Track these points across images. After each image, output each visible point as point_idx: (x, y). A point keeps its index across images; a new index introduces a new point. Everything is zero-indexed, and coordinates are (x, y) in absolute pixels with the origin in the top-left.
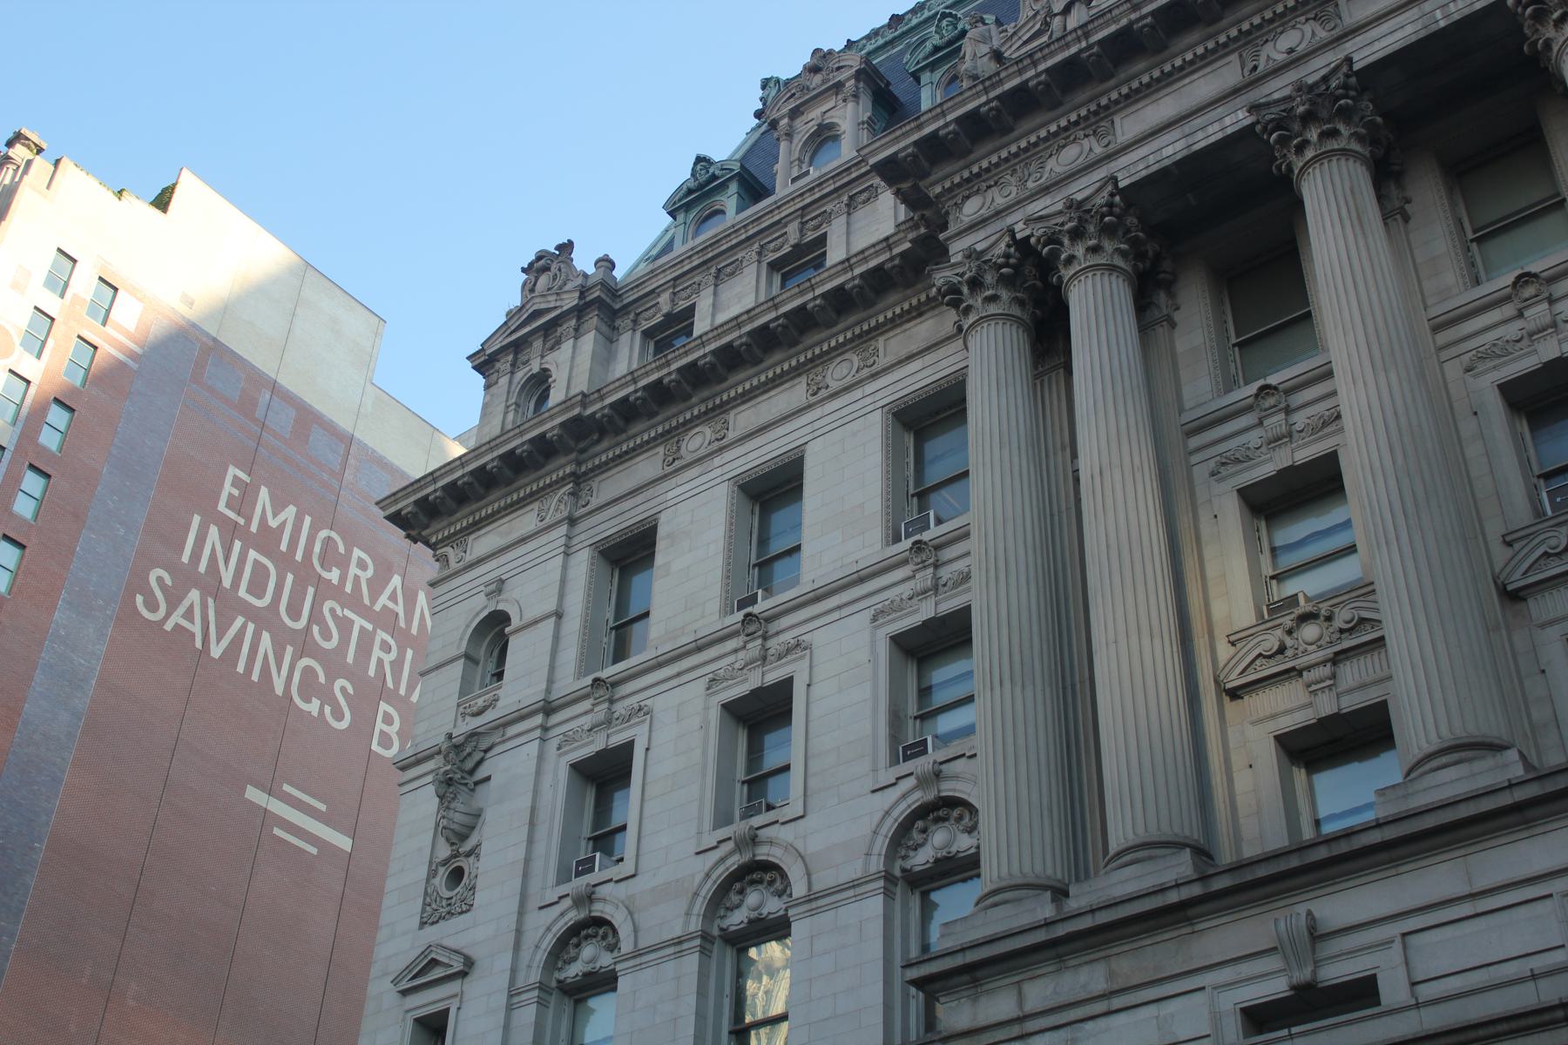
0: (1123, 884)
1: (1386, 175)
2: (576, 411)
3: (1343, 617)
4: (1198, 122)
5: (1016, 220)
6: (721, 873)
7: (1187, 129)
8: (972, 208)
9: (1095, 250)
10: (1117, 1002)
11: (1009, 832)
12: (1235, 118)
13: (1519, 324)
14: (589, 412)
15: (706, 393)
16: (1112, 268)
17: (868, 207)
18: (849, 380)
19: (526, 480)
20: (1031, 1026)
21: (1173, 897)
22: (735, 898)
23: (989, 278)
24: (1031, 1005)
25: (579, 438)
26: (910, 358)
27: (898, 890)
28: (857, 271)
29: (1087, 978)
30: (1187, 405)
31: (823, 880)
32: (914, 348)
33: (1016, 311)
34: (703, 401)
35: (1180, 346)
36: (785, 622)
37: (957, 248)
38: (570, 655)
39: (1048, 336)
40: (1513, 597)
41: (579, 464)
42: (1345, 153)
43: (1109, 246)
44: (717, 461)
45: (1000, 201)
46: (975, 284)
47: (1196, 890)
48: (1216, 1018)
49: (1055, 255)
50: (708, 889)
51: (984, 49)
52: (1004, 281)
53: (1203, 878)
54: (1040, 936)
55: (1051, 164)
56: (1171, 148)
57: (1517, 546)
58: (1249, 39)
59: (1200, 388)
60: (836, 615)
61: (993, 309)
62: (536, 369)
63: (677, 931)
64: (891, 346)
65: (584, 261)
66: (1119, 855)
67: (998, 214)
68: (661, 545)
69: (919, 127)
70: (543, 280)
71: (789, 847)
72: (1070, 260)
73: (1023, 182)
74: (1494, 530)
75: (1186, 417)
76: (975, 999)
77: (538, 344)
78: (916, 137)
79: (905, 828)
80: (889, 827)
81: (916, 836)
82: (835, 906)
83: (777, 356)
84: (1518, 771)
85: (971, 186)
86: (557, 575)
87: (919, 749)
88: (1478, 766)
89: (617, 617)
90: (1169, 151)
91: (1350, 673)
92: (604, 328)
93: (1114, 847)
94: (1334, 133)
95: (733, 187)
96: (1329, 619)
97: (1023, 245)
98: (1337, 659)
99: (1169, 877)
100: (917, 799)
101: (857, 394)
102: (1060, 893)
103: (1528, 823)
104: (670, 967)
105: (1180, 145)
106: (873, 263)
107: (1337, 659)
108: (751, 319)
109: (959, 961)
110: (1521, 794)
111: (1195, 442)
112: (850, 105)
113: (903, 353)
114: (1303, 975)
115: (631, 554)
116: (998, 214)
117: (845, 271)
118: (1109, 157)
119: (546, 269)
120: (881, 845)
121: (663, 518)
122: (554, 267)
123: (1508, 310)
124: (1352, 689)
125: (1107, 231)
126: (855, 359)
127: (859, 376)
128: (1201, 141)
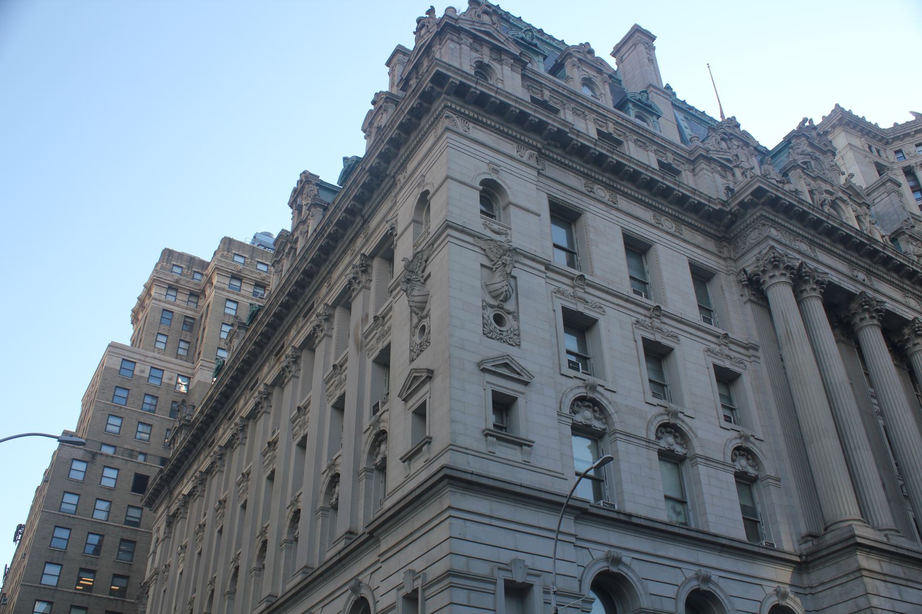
2: (567, 130)
7: (841, 277)
14: (570, 135)
15: (612, 177)
19: (516, 129)
26: (698, 247)
31: (710, 455)
34: (609, 179)
44: (614, 212)
45: (783, 241)
55: (798, 243)
60: (688, 336)
71: (690, 428)
83: (646, 193)
101: (677, 241)
106: (702, 201)
117: (692, 192)
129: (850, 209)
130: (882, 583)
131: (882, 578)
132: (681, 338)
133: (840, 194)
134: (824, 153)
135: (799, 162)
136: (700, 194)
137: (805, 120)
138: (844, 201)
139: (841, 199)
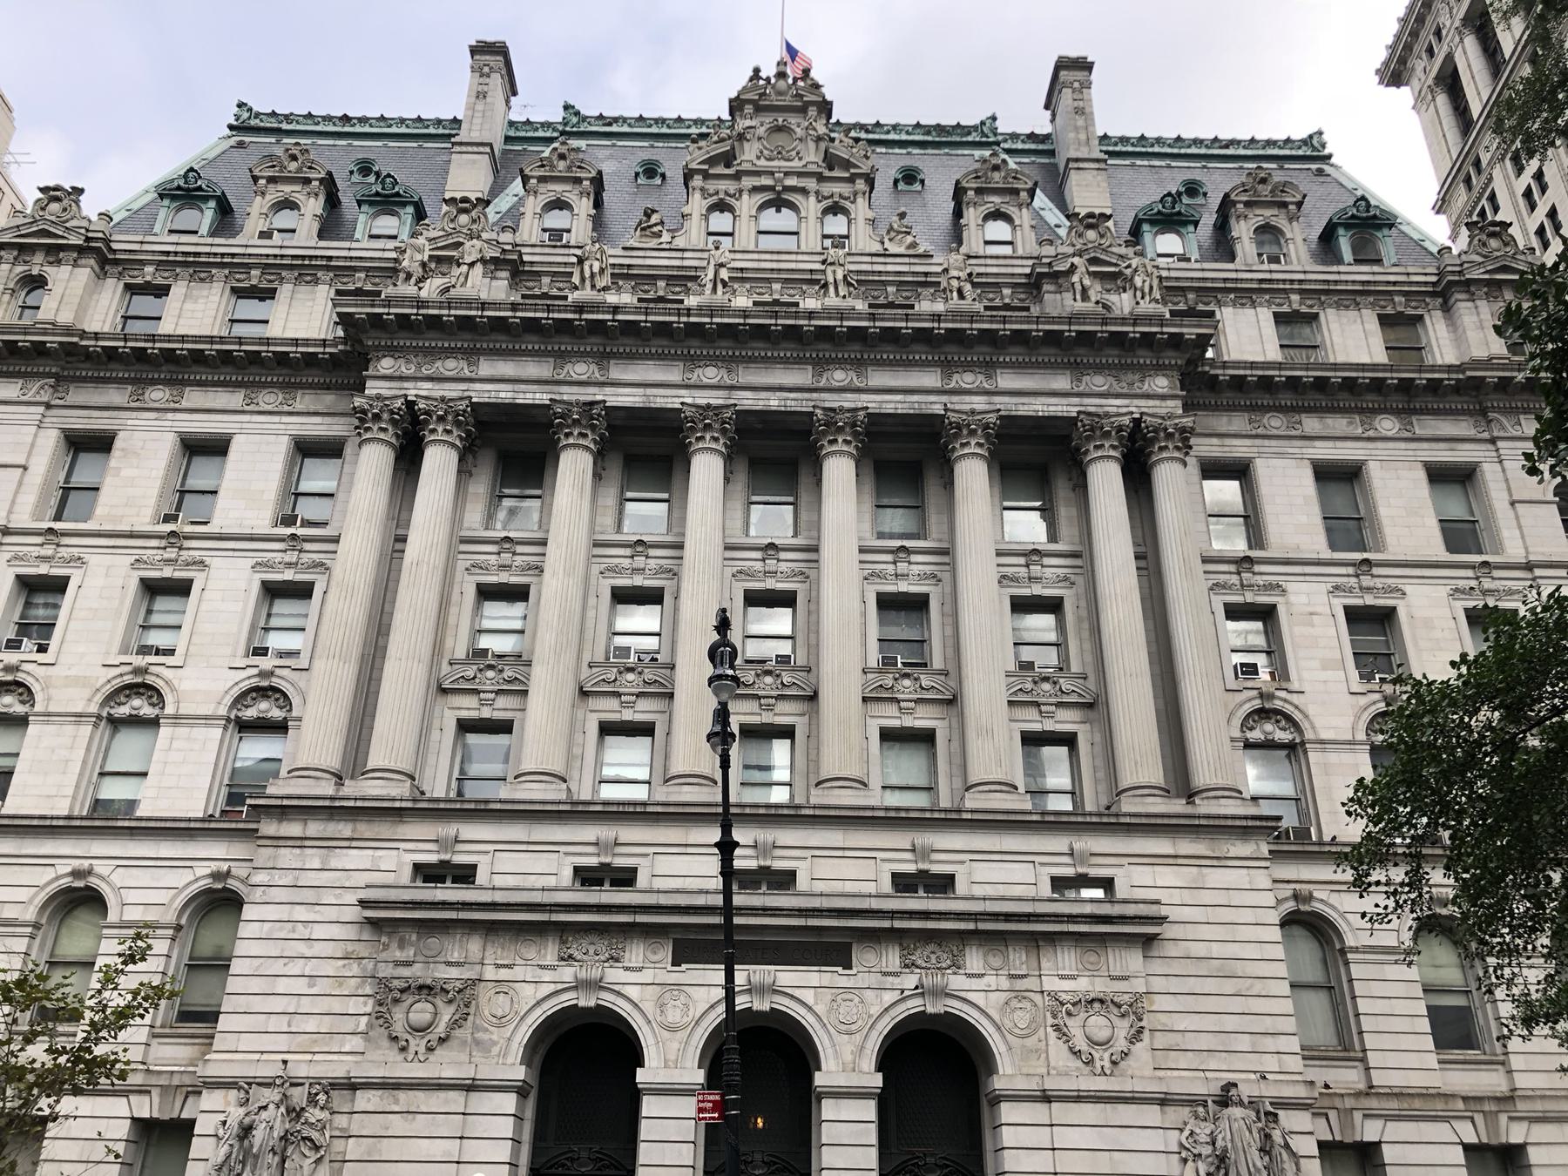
0: (372, 788)
1: (600, 456)
2: (75, 339)
3: (508, 673)
4: (523, 387)
5: (413, 390)
6: (118, 683)
8: (386, 365)
9: (448, 432)
10: (354, 844)
11: (316, 740)
12: (540, 396)
13: (629, 561)
14: (84, 343)
16: (453, 445)
17: (309, 288)
18: (269, 408)
20: (307, 843)
21: (397, 804)
22: (123, 699)
23: (385, 416)
24: (308, 834)
25: (68, 354)
26: (316, 414)
27: (231, 726)
28: (300, 349)
29: (344, 829)
30: (466, 525)
32: (320, 408)
33: (394, 441)
35: (471, 489)
36: (194, 544)
37: (373, 388)
38: (28, 499)
39: (408, 460)
40: (584, 694)
41: (63, 369)
42: (587, 448)
43: (455, 433)
44: (170, 415)
46: (377, 417)
47: (409, 805)
48: (400, 864)
49: (426, 422)
50: (108, 689)
51: (419, 257)
52: (393, 422)
53: (414, 800)
54: (327, 803)
55: (439, 364)
56: (504, 394)
57: (595, 670)
58: (562, 357)
59: (474, 518)
61: (382, 436)
62: (35, 272)
63: (79, 708)
64: (304, 401)
65: (90, 207)
66: (373, 771)
67: (401, 378)
68: (115, 452)
69: (373, 306)
70: (54, 207)
72: (433, 431)
73: (419, 366)
74: (587, 658)
75: (463, 533)
76: (280, 821)
77: (39, 258)
78: (369, 310)
79: (244, 694)
80: (236, 692)
81: (249, 701)
82: (191, 726)
84: (563, 796)
85: (392, 351)
86: (29, 439)
87: (262, 651)
88: (548, 786)
89: (67, 481)
90: (503, 395)
91: (502, 702)
92: (97, 268)
93: (370, 765)
94: (584, 436)
95: (212, 204)
96: (501, 671)
97: (410, 405)
98: (498, 692)
99: (394, 793)
100: (254, 682)
101: (276, 419)
102: (339, 778)
103: (560, 819)
104: (69, 729)
105: (509, 395)
106: (311, 350)
107: (498, 692)
108: (222, 343)
109: (278, 802)
110: (562, 807)
111: (464, 547)
112: (312, 200)
113: (312, 408)
114: (446, 857)
115: (90, 444)
116: (401, 378)
118: (471, 380)
119: (58, 199)
120: (228, 700)
121: (121, 435)
122: (66, 202)
123: (628, 552)
124: (501, 709)
125: (458, 424)
126: (281, 396)
127: (280, 409)
128: (522, 399)
129: (812, 199)
130: (298, 851)
131: (298, 843)
132: (208, 561)
133: (791, 182)
134: (802, 110)
135: (694, 166)
136: (307, 342)
137: (757, 71)
138: (804, 191)
139: (787, 189)
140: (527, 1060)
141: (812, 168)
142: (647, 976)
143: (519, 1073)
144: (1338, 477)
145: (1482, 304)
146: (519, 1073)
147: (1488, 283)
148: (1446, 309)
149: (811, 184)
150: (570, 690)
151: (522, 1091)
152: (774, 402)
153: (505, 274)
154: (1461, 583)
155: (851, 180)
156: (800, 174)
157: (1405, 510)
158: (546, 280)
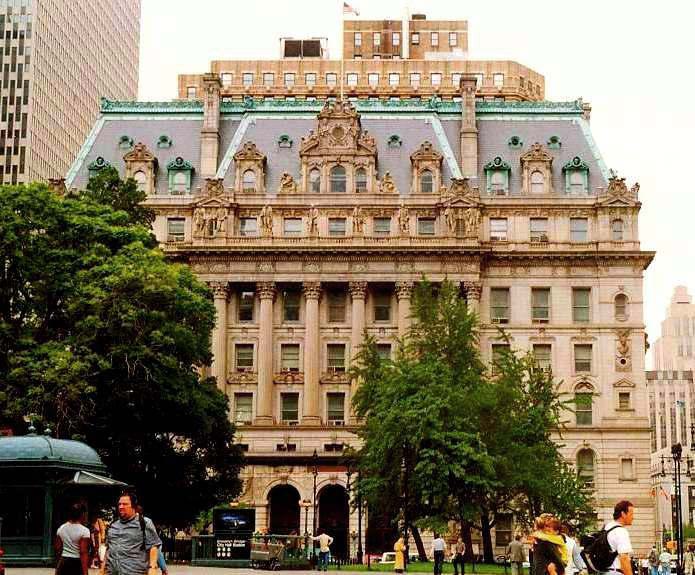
140: (268, 499)
141: (351, 151)
142: (301, 475)
143: (267, 503)
144: (541, 292)
145: (607, 216)
146: (267, 503)
147: (611, 208)
148: (596, 215)
149: (350, 158)
150: (271, 383)
151: (267, 506)
152: (334, 279)
153: (232, 212)
154: (575, 335)
155: (368, 156)
156: (347, 155)
157: (561, 302)
158: (248, 211)
